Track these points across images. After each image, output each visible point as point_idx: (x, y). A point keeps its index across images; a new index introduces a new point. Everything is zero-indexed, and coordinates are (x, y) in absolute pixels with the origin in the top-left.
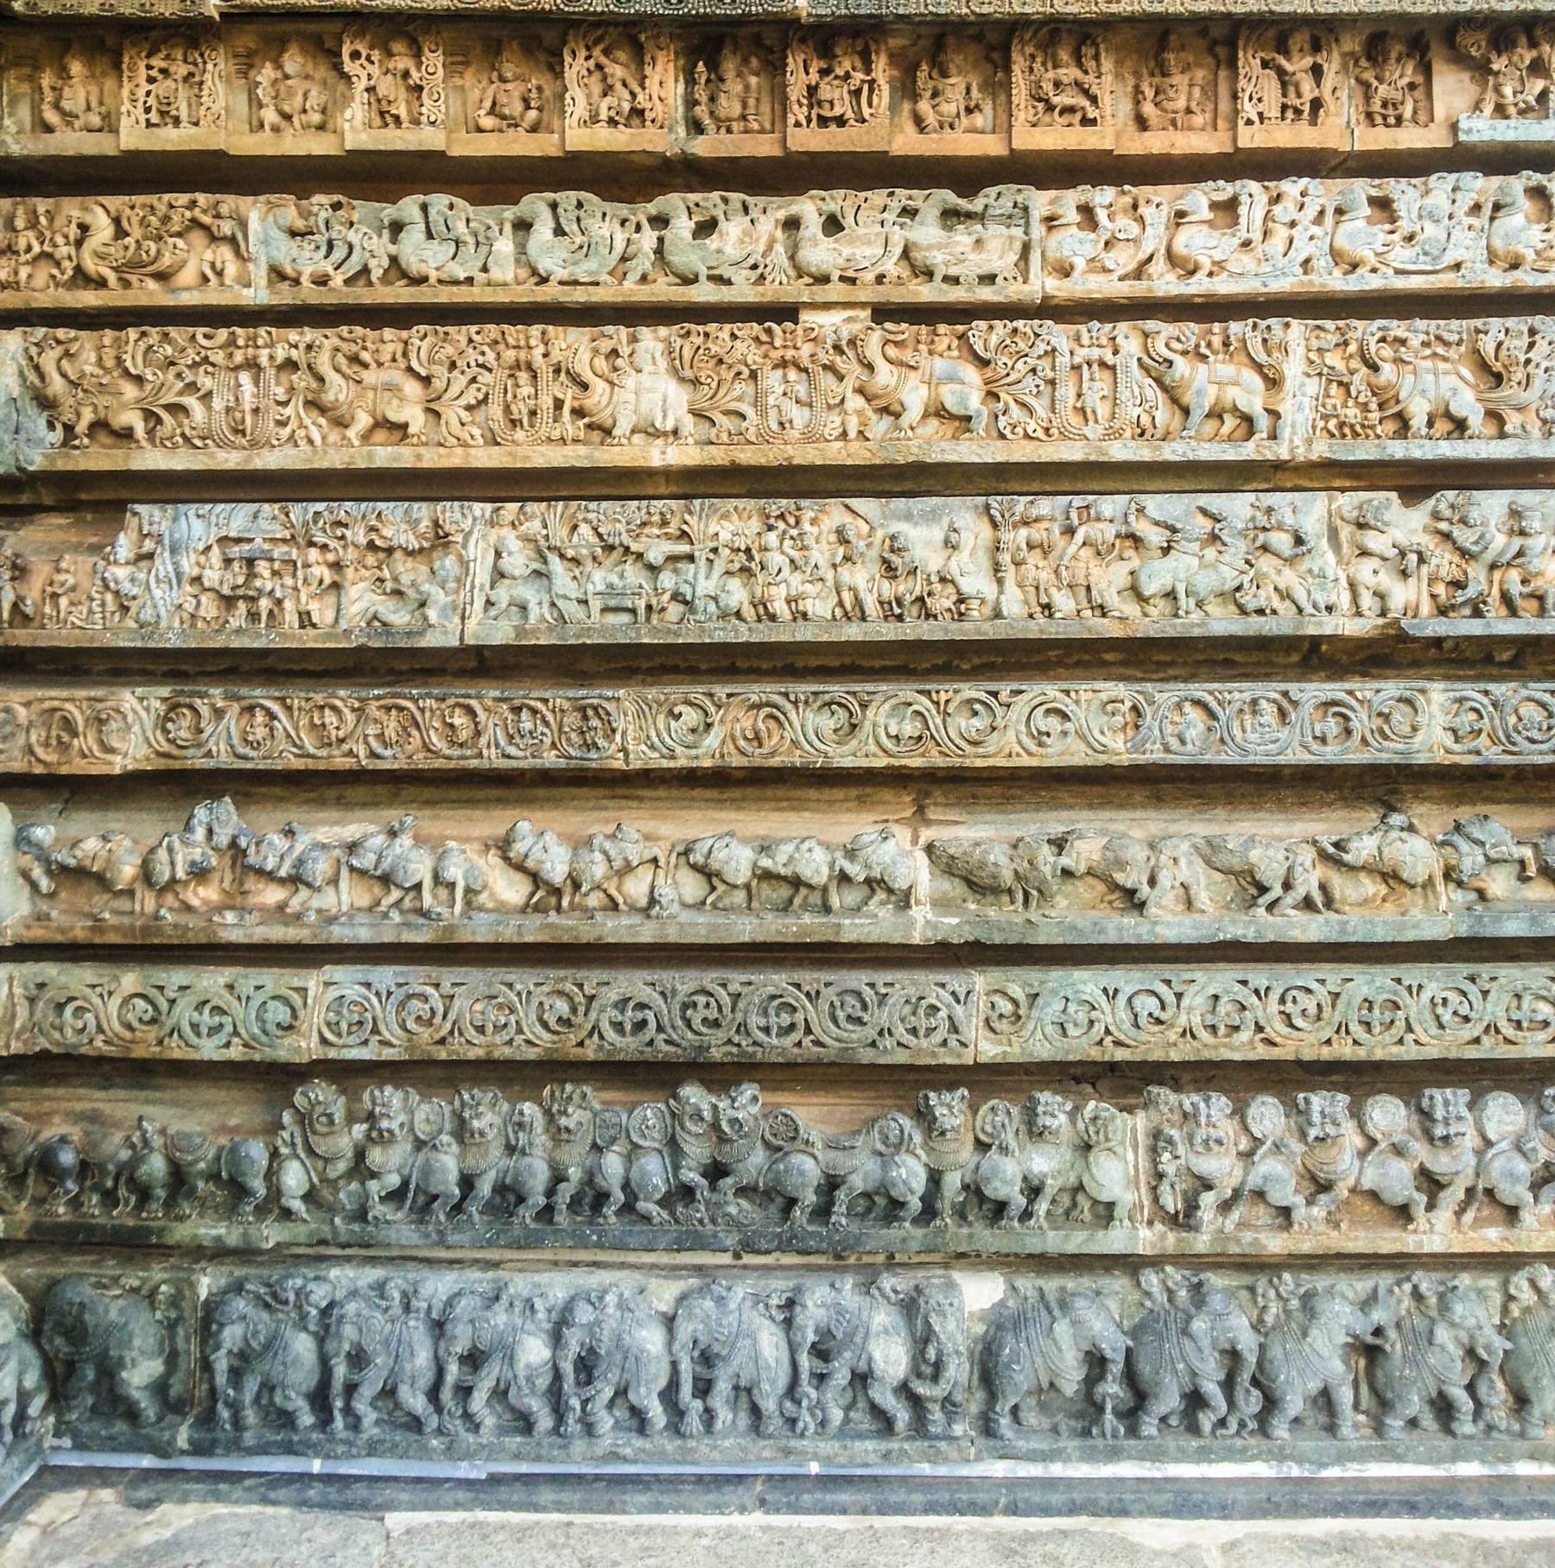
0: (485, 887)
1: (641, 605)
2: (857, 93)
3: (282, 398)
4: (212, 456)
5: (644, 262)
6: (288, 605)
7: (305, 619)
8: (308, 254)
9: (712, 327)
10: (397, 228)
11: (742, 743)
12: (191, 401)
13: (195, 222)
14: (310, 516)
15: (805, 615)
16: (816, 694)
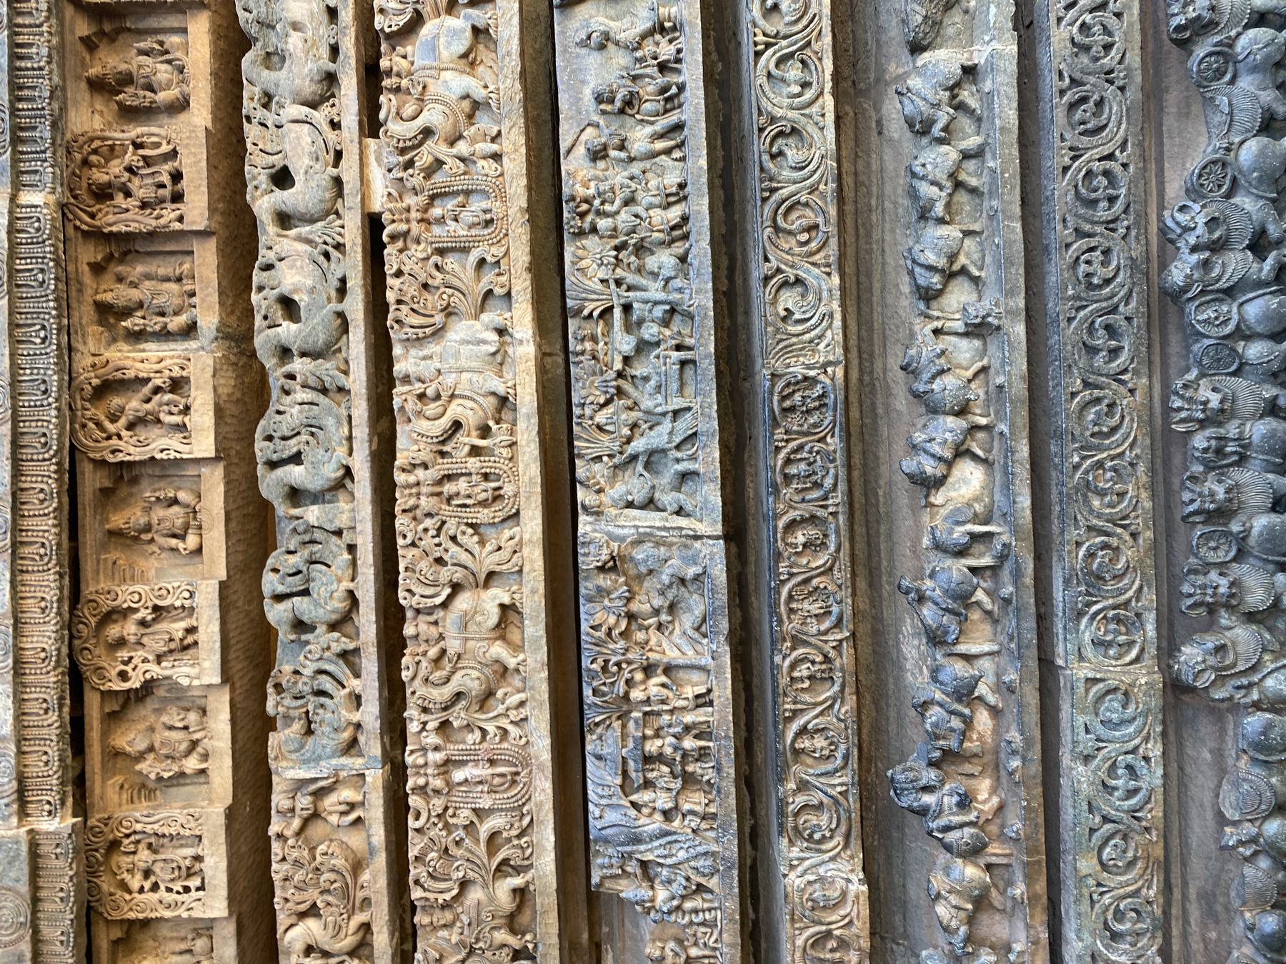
0: (969, 505)
1: (676, 355)
2: (148, 161)
3: (478, 734)
4: (540, 805)
5: (327, 369)
6: (689, 718)
7: (703, 700)
8: (329, 715)
9: (391, 296)
10: (300, 626)
11: (814, 245)
12: (484, 829)
13: (298, 834)
14: (597, 700)
15: (682, 186)
16: (762, 169)
